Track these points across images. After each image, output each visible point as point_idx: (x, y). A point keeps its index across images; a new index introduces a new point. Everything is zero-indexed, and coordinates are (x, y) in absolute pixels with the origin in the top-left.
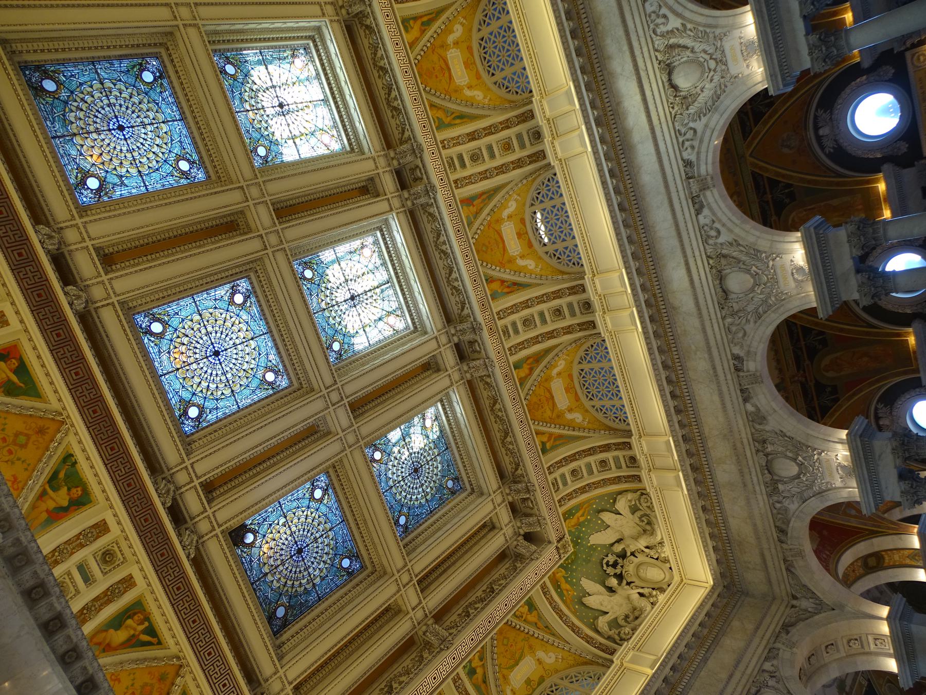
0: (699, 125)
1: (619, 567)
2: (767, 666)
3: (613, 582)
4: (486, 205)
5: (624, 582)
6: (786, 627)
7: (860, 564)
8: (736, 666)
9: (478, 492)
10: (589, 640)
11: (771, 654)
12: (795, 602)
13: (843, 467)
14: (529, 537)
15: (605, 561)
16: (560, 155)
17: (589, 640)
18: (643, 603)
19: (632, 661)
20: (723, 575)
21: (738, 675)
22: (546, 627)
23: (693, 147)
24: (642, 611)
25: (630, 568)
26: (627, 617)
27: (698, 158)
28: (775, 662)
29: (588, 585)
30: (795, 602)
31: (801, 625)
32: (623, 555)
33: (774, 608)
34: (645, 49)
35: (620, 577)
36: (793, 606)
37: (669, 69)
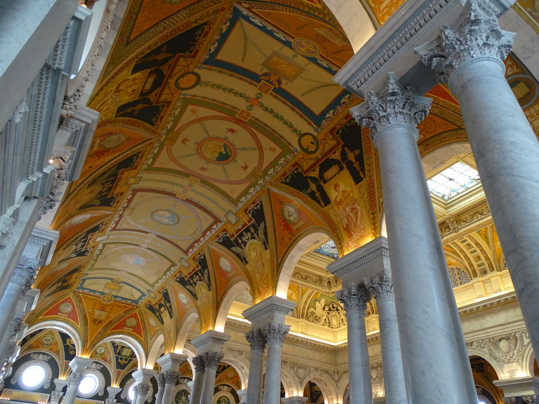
0: (486, 349)
2: (312, 369)
3: (327, 309)
4: (449, 252)
6: (326, 372)
8: (309, 359)
10: (304, 308)
11: (316, 369)
13: (377, 394)
14: (329, 282)
16: (475, 285)
18: (323, 321)
19: (301, 325)
21: (307, 360)
23: (477, 346)
24: (319, 322)
25: (333, 313)
26: (317, 317)
27: (473, 349)
31: (329, 377)
32: (337, 310)
33: (333, 366)
34: (516, 328)
35: (330, 310)
37: (508, 339)
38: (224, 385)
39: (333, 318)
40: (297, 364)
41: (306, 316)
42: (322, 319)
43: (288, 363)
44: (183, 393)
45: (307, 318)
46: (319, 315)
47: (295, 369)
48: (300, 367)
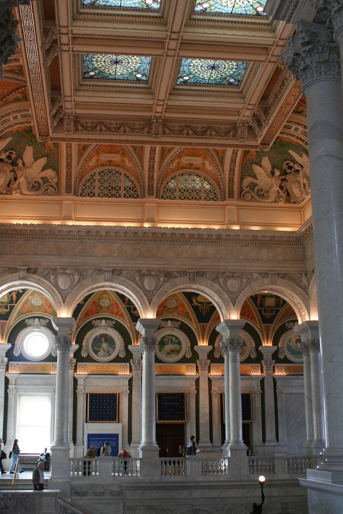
1: (290, 171)
2: (255, 275)
3: (277, 173)
5: (283, 177)
6: (284, 276)
9: (242, 95)
10: (231, 181)
12: (303, 275)
14: (250, 128)
15: (288, 162)
17: (231, 181)
18: (273, 196)
22: (222, 158)
26: (262, 190)
28: (260, 278)
29: (266, 161)
30: (303, 275)
32: (298, 171)
35: (284, 173)
39: (293, 185)
40: (224, 273)
41: (241, 192)
42: (271, 191)
43: (208, 275)
44: (103, 339)
45: (241, 196)
47: (221, 280)
48: (232, 276)
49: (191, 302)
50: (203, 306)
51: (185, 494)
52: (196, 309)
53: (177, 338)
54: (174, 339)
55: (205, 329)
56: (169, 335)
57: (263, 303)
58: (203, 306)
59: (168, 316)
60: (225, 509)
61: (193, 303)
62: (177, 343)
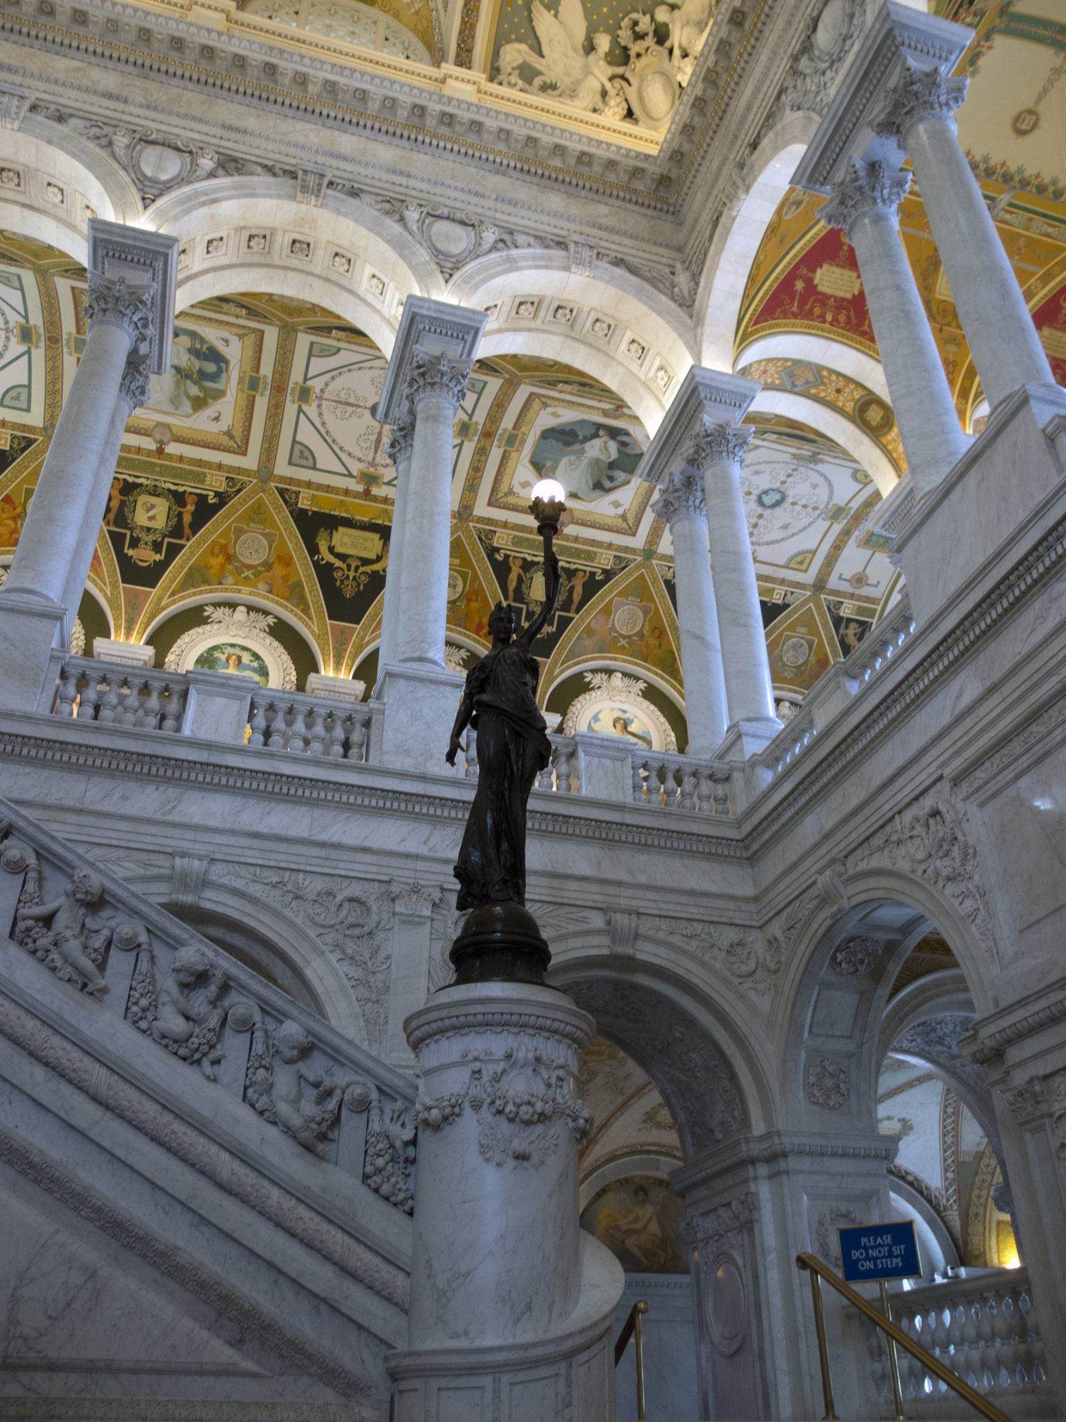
2: (521, 239)
3: (603, 43)
5: (620, 70)
7: (857, 397)
12: (679, 266)
15: (634, 16)
20: (677, 156)
26: (554, 87)
30: (679, 266)
36: (673, 273)
38: (233, 606)
46: (564, 83)
49: (313, 550)
50: (349, 566)
51: (146, 800)
52: (325, 573)
53: (257, 657)
54: (246, 658)
55: (348, 640)
56: (233, 645)
57: (524, 589)
58: (349, 566)
59: (239, 591)
60: (338, 900)
61: (318, 552)
62: (254, 670)
